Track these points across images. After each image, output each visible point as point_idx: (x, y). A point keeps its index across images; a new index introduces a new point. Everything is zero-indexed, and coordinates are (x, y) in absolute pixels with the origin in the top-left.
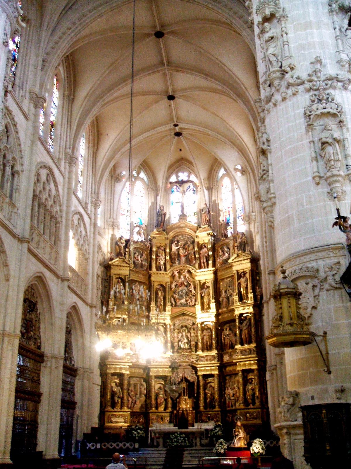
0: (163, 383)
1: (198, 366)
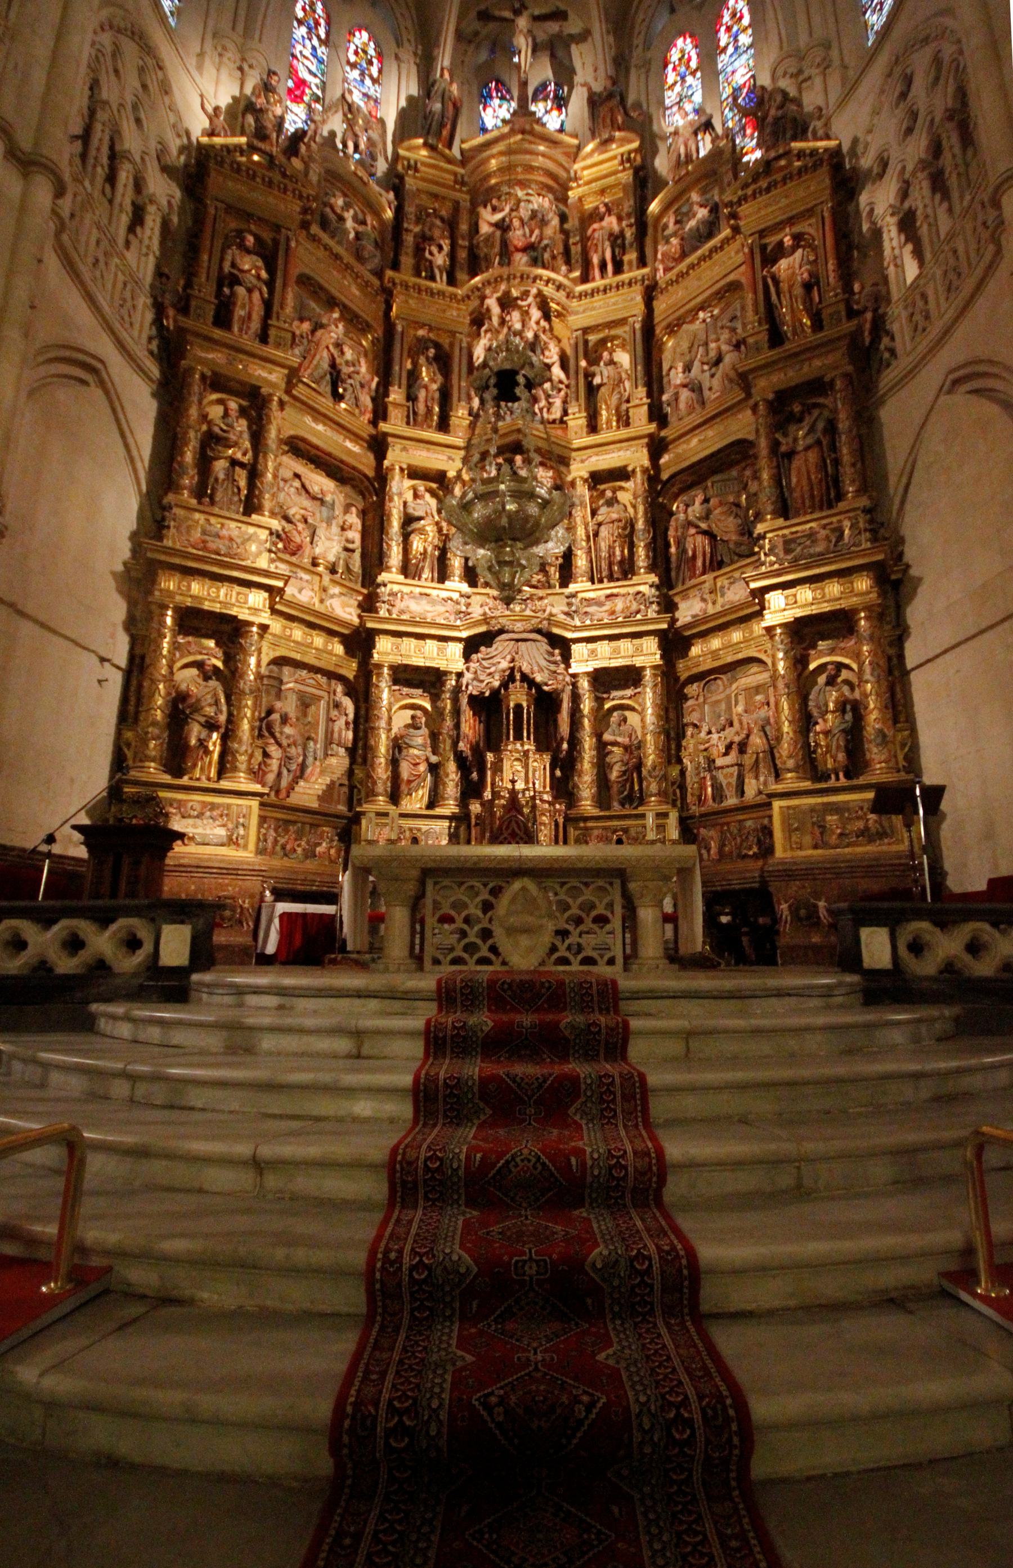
0: (428, 706)
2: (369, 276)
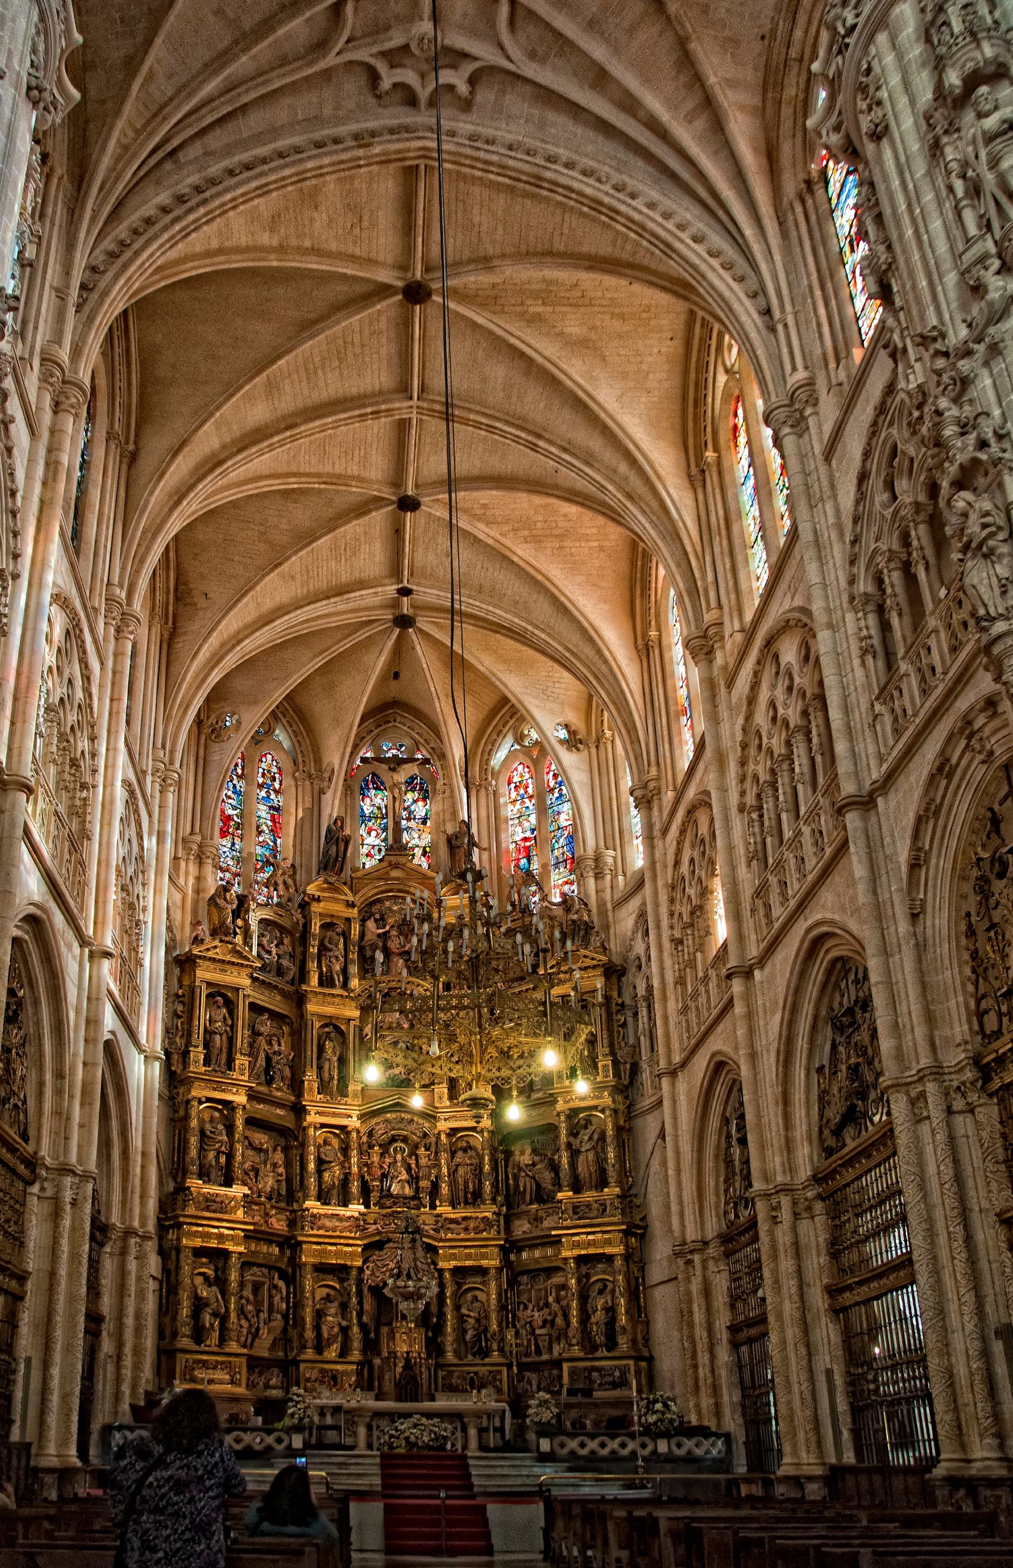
2: (289, 988)
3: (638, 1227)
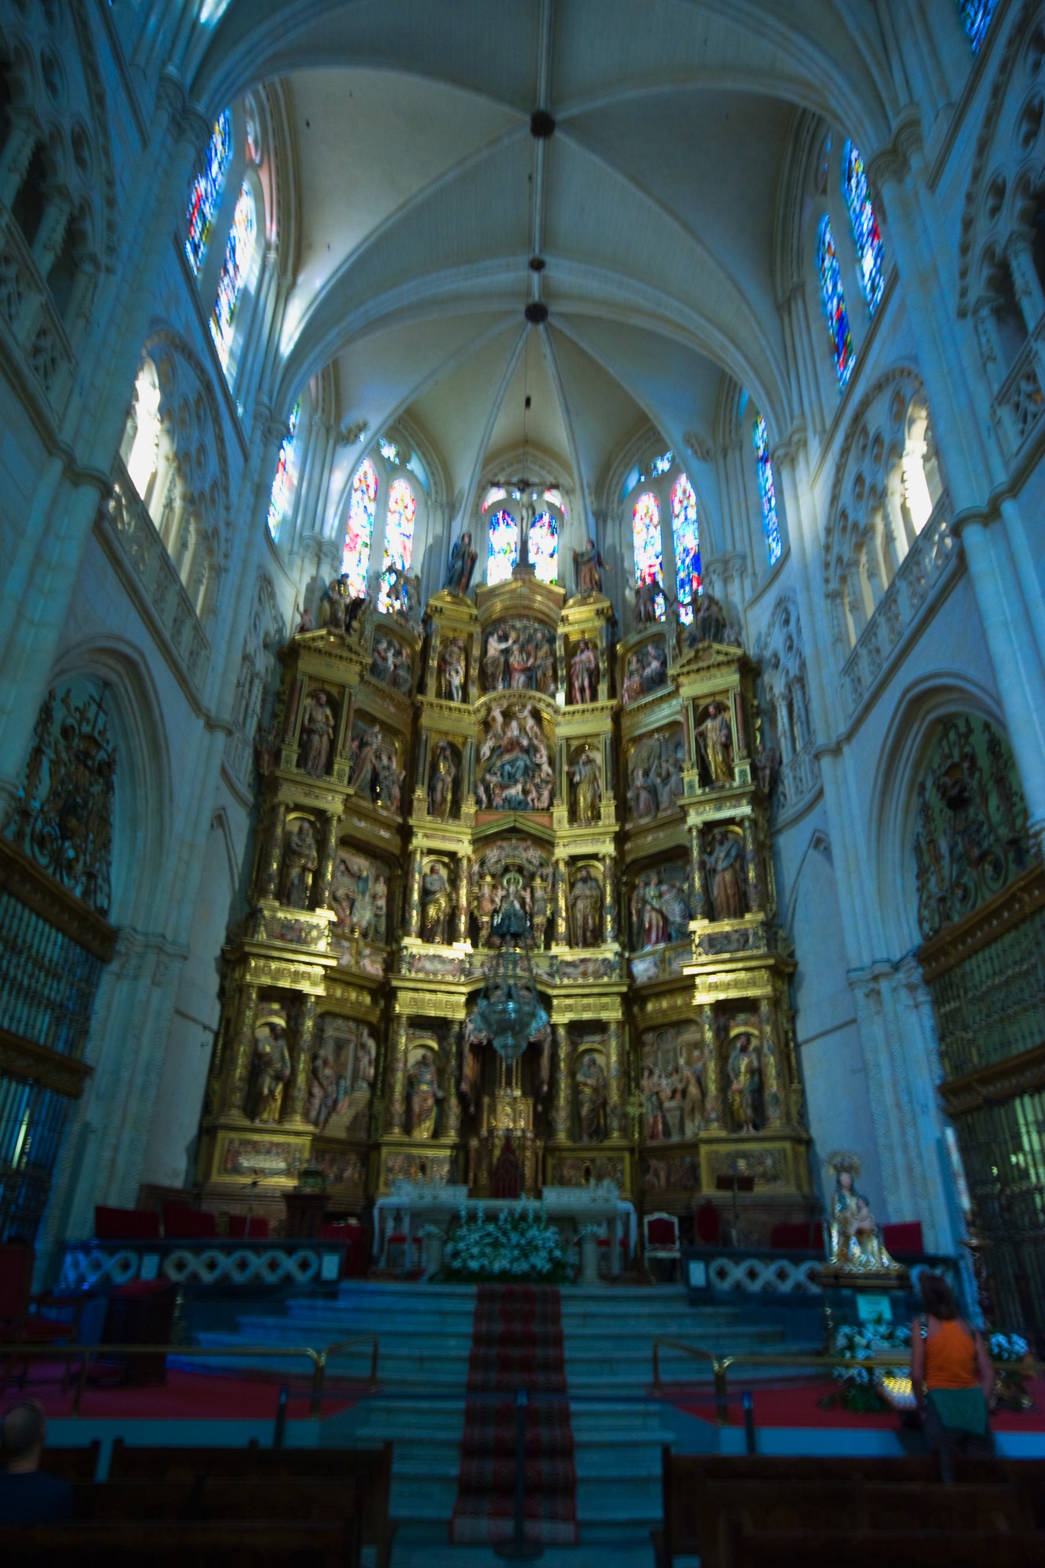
0: (435, 1045)
1: (555, 992)
3: (788, 965)
